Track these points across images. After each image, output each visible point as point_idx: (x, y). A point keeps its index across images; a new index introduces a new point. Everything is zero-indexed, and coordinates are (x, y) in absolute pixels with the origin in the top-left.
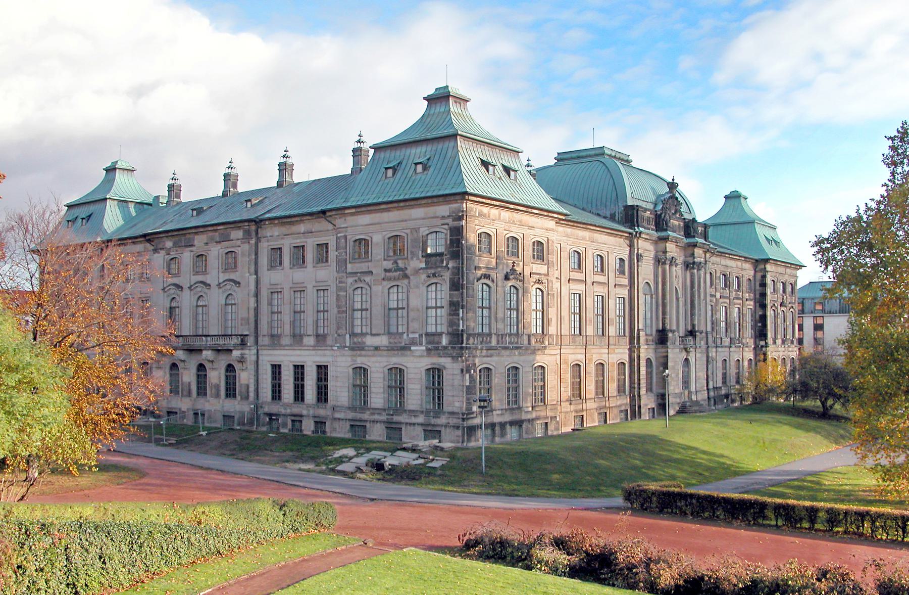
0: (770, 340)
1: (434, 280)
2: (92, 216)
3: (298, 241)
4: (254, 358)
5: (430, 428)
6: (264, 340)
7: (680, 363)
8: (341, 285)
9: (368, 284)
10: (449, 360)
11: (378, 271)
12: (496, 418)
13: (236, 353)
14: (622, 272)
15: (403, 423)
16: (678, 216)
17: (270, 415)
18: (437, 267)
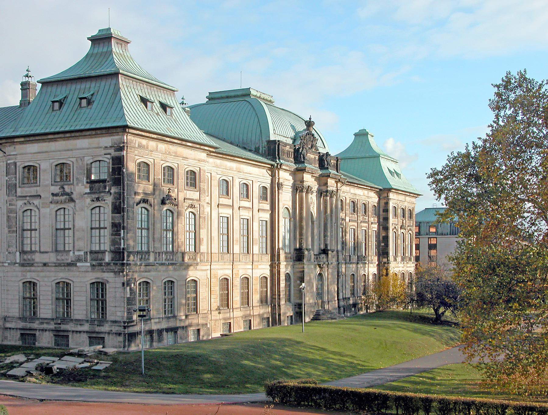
0: (391, 258)
1: (98, 204)
5: (94, 335)
8: (11, 207)
9: (36, 206)
10: (112, 274)
11: (46, 195)
15: (70, 331)
16: (314, 150)
18: (100, 192)
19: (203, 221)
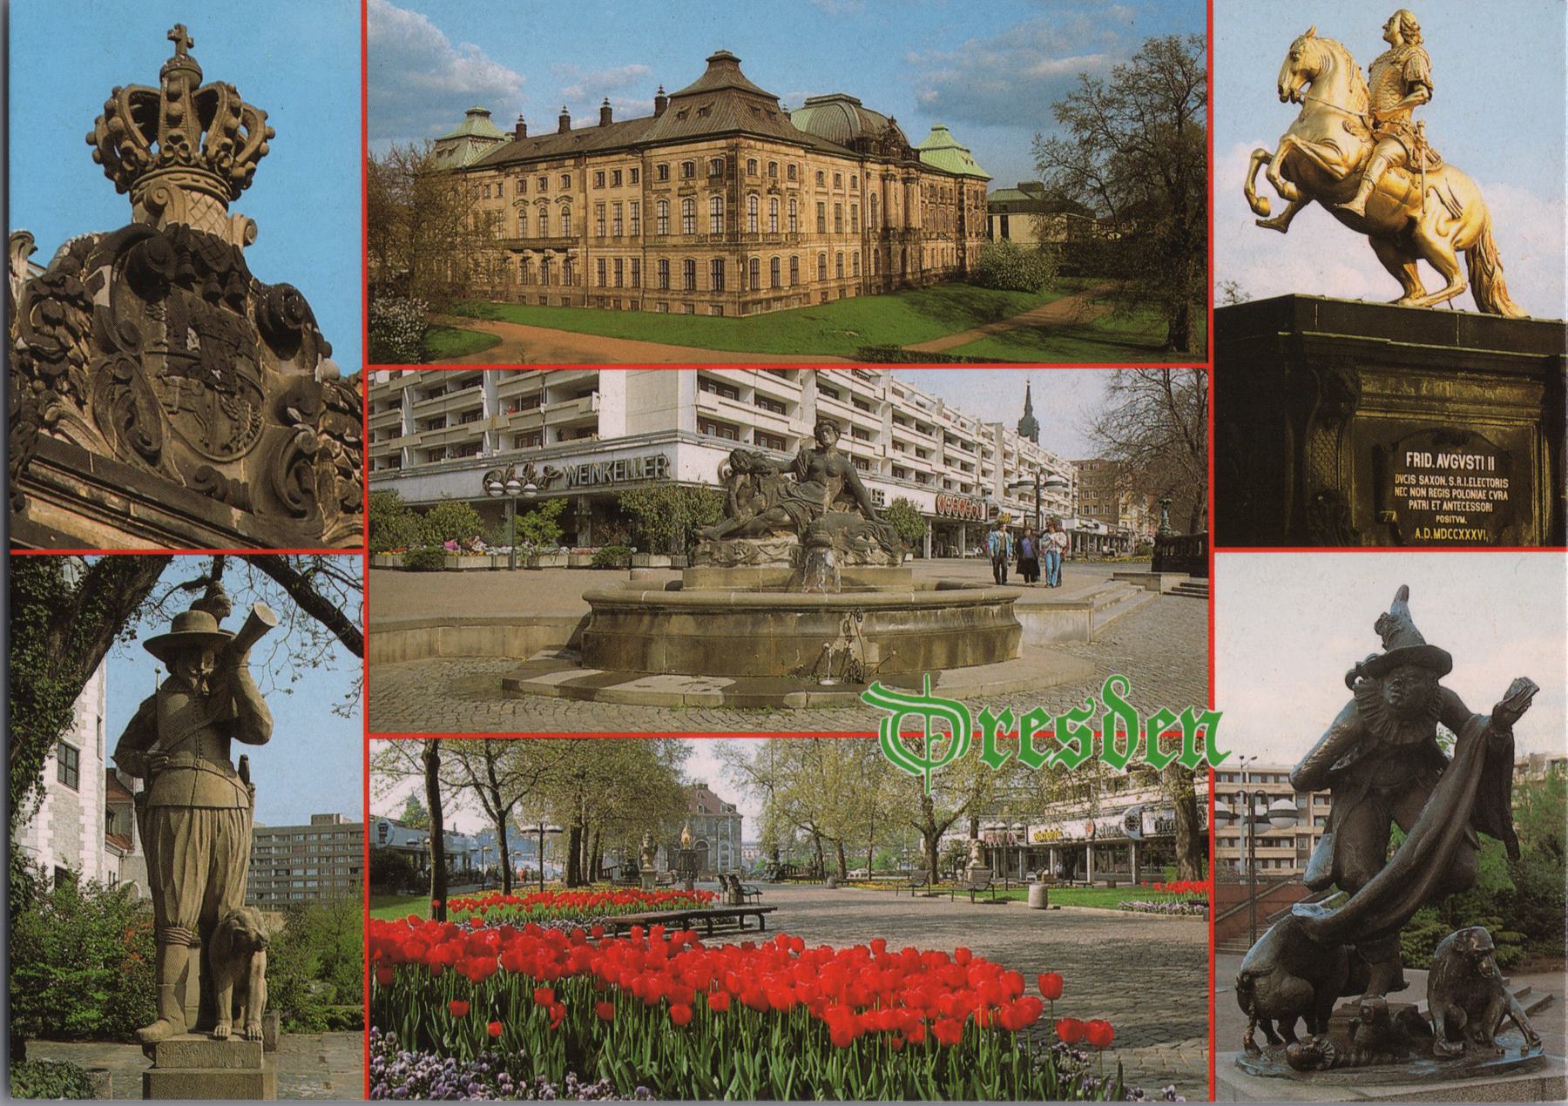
11: (675, 189)
12: (762, 295)
14: (854, 186)
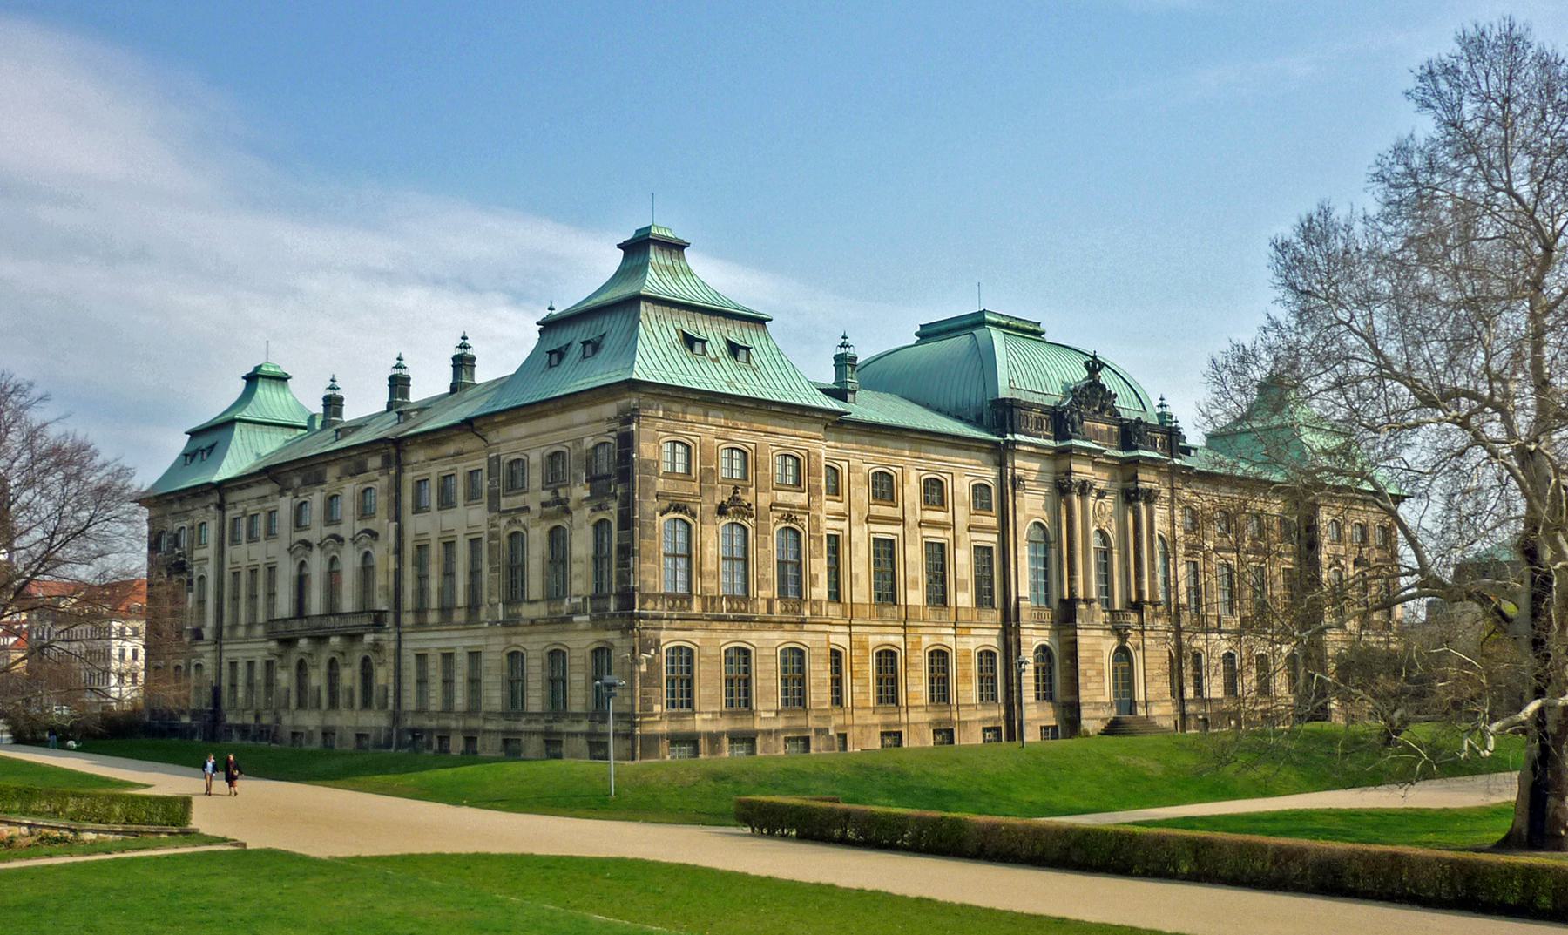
1: (600, 516)
2: (215, 448)
3: (448, 467)
4: (393, 646)
5: (595, 740)
6: (408, 619)
7: (1106, 653)
9: (523, 526)
11: (535, 507)
12: (701, 723)
13: (369, 638)
17: (413, 731)
19: (818, 543)
